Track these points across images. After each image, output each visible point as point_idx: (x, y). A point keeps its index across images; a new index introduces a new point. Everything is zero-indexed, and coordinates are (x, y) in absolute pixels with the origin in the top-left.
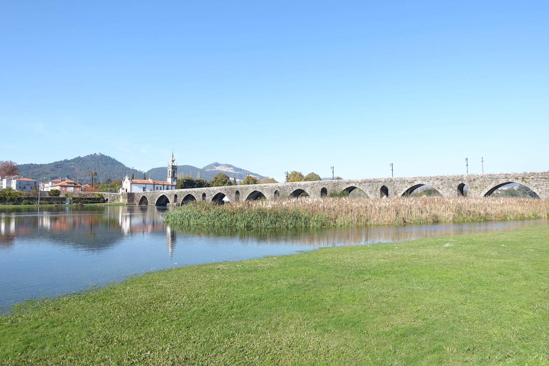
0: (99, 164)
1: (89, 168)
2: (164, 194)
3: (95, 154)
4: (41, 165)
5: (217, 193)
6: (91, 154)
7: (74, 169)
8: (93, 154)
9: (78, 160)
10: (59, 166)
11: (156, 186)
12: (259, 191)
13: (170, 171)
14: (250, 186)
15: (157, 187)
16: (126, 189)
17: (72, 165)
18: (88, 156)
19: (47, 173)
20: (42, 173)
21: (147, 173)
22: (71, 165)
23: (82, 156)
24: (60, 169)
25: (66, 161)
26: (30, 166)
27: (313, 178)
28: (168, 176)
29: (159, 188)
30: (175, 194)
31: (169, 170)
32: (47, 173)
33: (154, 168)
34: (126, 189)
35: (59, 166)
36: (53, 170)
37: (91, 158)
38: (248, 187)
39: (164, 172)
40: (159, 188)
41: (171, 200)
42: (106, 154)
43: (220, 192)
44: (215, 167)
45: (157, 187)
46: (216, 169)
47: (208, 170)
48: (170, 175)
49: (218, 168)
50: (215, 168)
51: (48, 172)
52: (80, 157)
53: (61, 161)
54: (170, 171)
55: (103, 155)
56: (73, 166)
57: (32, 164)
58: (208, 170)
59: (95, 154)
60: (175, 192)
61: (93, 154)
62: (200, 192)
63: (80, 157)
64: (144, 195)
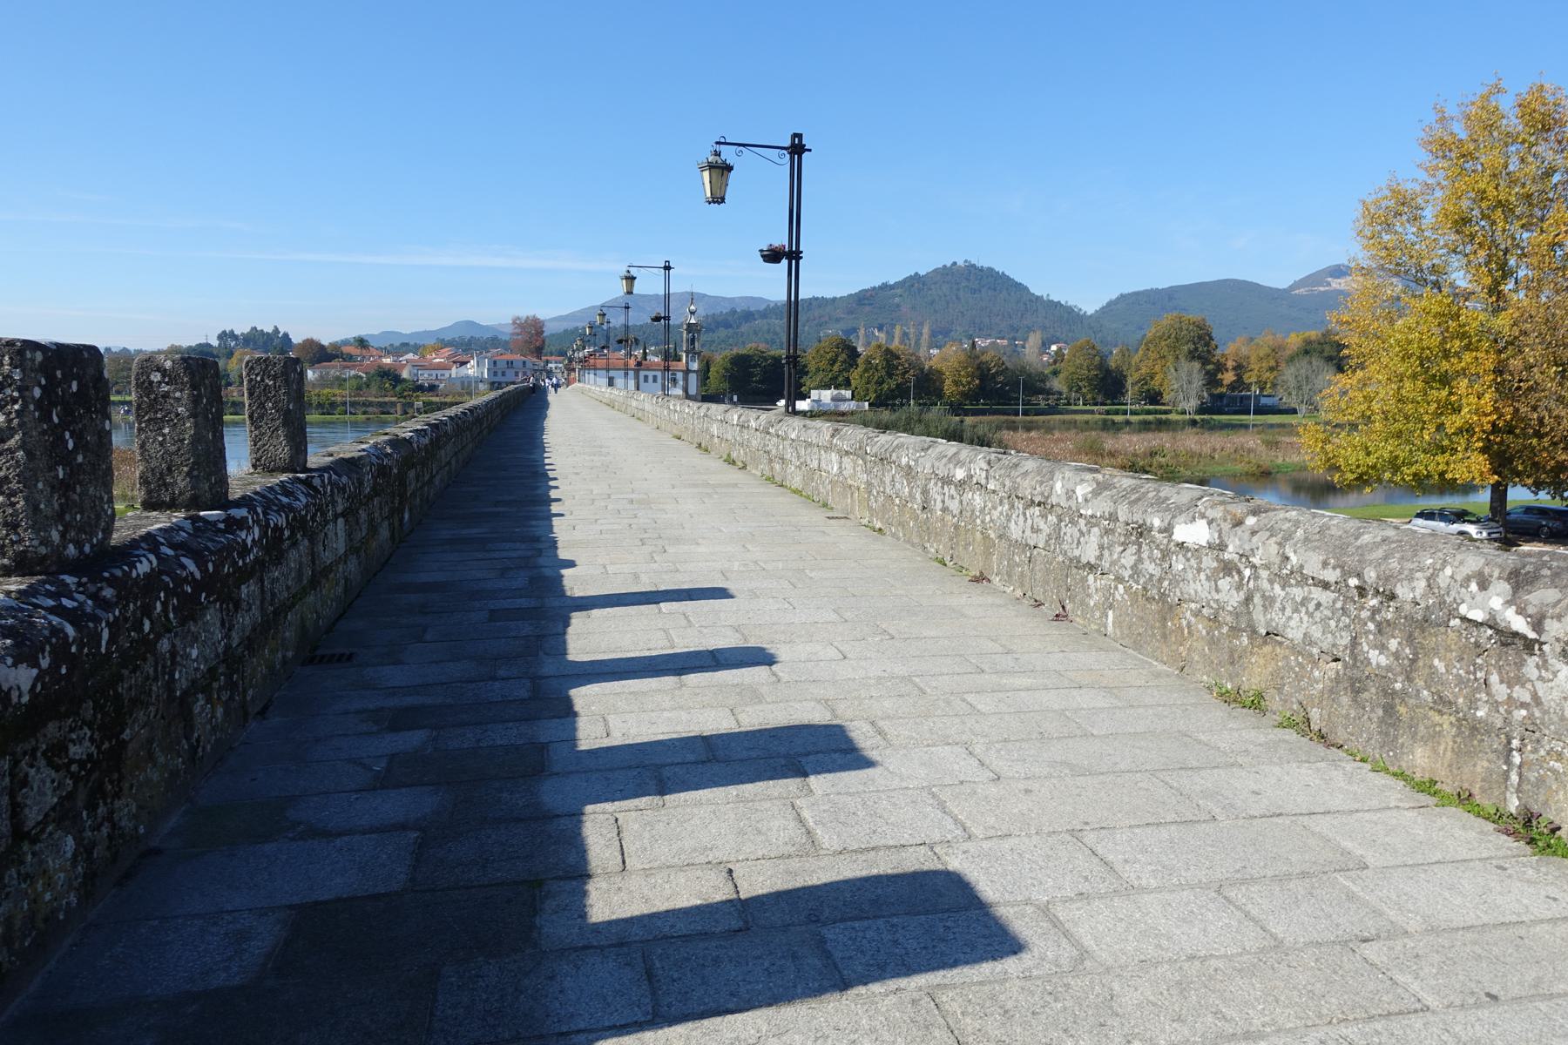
0: (958, 290)
1: (933, 302)
3: (955, 263)
4: (834, 299)
6: (945, 266)
7: (898, 306)
8: (949, 265)
9: (914, 283)
10: (866, 302)
11: (642, 374)
15: (646, 378)
17: (894, 296)
18: (936, 271)
19: (838, 320)
20: (827, 319)
21: (1103, 308)
22: (894, 296)
23: (922, 273)
24: (867, 308)
25: (885, 287)
26: (810, 304)
27: (1169, 337)
29: (650, 379)
32: (838, 320)
33: (1126, 291)
35: (866, 302)
36: (850, 312)
37: (943, 274)
39: (1154, 304)
40: (650, 379)
42: (983, 262)
44: (1329, 279)
45: (646, 378)
46: (1334, 285)
47: (1302, 290)
49: (1337, 284)
50: (1329, 284)
51: (842, 316)
52: (917, 273)
53: (874, 288)
55: (974, 266)
56: (897, 300)
57: (817, 299)
58: (1302, 291)
59: (955, 263)
61: (949, 265)
63: (917, 273)
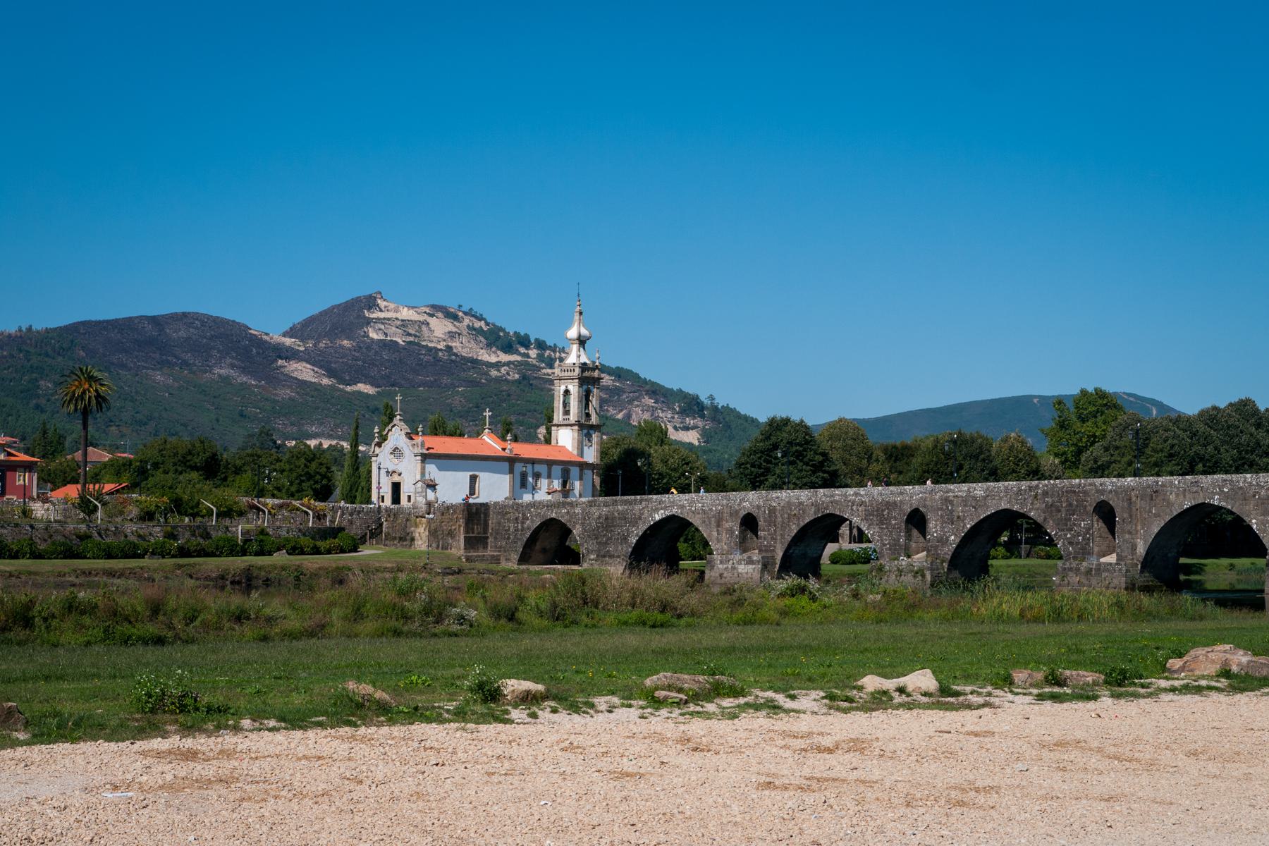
2: (675, 511)
5: (992, 511)
12: (1223, 504)
13: (567, 392)
14: (1171, 482)
16: (396, 487)
28: (558, 416)
30: (743, 513)
31: (563, 388)
34: (396, 487)
38: (1163, 486)
41: (720, 540)
43: (1004, 505)
48: (567, 412)
54: (567, 392)
60: (747, 504)
62: (891, 505)
64: (554, 515)
